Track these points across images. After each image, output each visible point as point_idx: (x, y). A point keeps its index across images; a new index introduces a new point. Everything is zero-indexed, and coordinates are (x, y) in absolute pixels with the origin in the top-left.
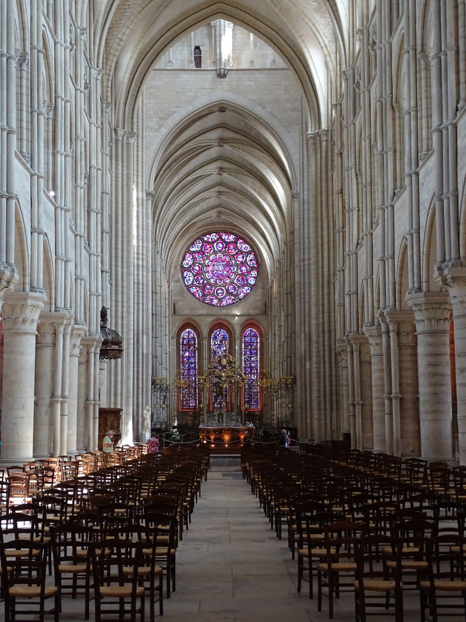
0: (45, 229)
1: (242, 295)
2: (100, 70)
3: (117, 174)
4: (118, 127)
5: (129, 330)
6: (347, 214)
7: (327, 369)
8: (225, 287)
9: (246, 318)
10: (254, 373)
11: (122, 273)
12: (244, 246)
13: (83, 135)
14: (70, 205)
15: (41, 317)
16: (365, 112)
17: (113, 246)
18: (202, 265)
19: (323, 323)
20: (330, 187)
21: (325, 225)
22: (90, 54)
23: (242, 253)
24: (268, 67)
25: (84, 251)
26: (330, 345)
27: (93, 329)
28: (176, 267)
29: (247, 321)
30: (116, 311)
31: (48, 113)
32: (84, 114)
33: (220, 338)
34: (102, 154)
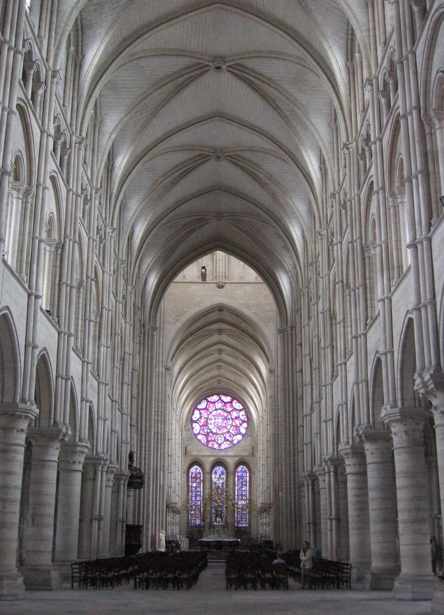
0: (90, 398)
1: (235, 442)
2: (134, 287)
3: (143, 355)
4: (145, 322)
5: (149, 468)
6: (304, 387)
7: (293, 497)
8: (223, 435)
11: (146, 427)
13: (120, 332)
14: (108, 381)
15: (86, 459)
16: (314, 319)
17: (140, 407)
18: (207, 419)
19: (290, 464)
20: (294, 367)
21: (291, 393)
22: (127, 275)
23: (236, 410)
24: (253, 281)
25: (118, 412)
26: (294, 480)
27: (123, 467)
28: (187, 420)
30: (141, 455)
31: (96, 319)
32: (121, 316)
33: (219, 473)
34: (134, 343)
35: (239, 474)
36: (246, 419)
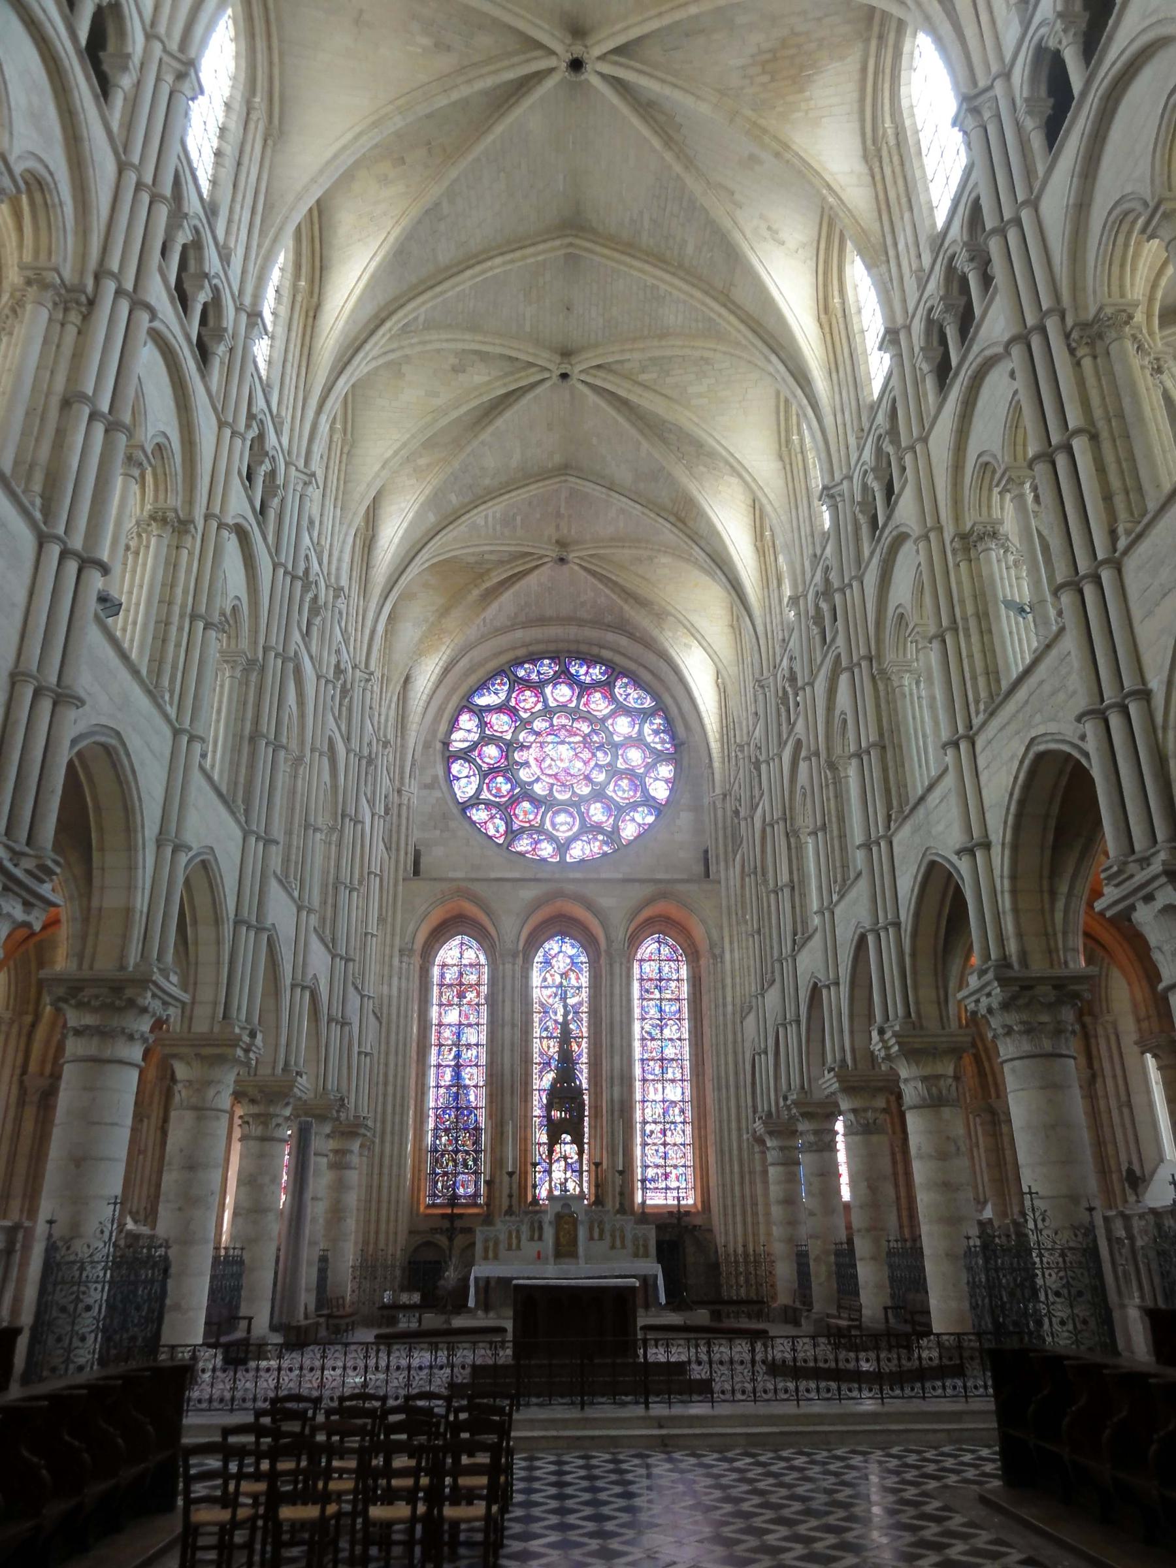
1: (629, 831)
8: (576, 805)
9: (648, 890)
10: (673, 1081)
12: (634, 694)
18: (509, 744)
28: (427, 745)
29: (649, 901)
35: (646, 966)
36: (672, 750)
